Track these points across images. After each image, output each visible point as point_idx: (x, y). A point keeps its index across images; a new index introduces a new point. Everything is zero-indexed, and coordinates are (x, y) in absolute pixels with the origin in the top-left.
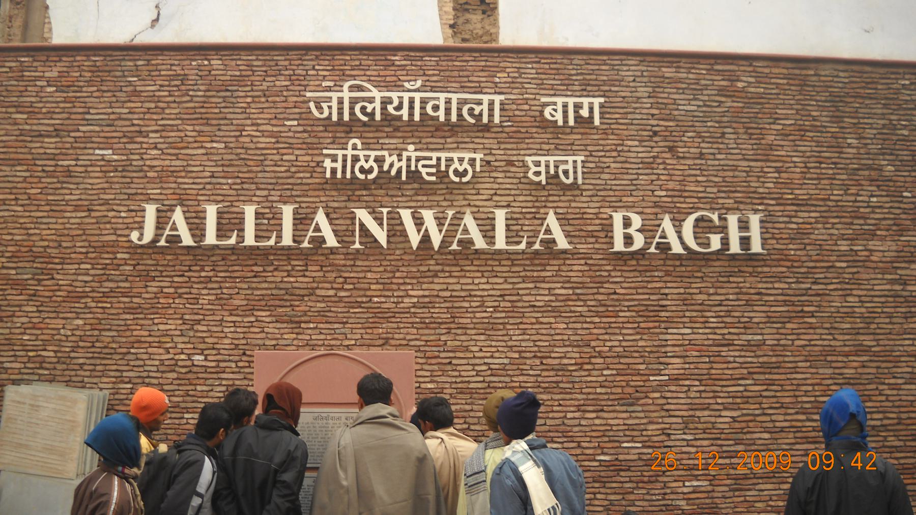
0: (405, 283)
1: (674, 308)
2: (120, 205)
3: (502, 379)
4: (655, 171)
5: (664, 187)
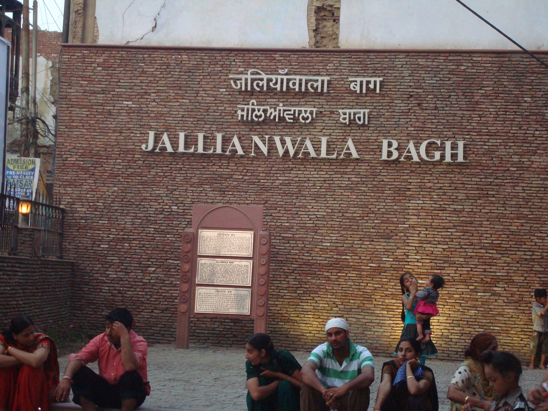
0: (276, 173)
1: (414, 190)
2: (136, 130)
3: (322, 222)
4: (409, 117)
5: (413, 126)
